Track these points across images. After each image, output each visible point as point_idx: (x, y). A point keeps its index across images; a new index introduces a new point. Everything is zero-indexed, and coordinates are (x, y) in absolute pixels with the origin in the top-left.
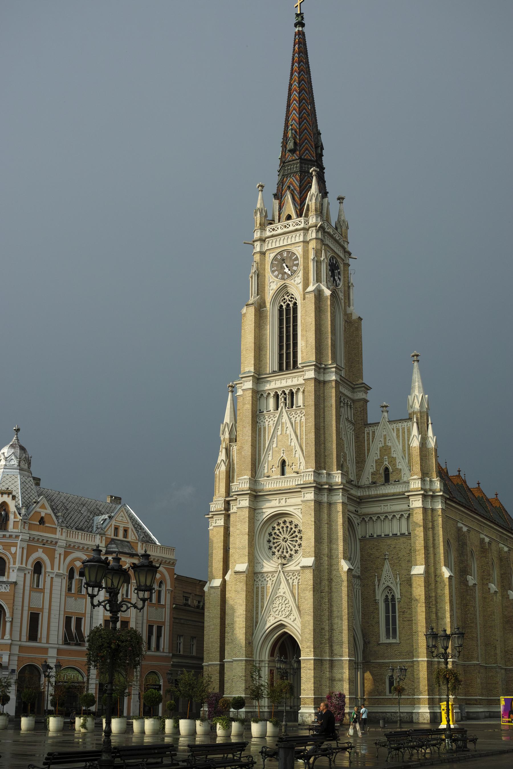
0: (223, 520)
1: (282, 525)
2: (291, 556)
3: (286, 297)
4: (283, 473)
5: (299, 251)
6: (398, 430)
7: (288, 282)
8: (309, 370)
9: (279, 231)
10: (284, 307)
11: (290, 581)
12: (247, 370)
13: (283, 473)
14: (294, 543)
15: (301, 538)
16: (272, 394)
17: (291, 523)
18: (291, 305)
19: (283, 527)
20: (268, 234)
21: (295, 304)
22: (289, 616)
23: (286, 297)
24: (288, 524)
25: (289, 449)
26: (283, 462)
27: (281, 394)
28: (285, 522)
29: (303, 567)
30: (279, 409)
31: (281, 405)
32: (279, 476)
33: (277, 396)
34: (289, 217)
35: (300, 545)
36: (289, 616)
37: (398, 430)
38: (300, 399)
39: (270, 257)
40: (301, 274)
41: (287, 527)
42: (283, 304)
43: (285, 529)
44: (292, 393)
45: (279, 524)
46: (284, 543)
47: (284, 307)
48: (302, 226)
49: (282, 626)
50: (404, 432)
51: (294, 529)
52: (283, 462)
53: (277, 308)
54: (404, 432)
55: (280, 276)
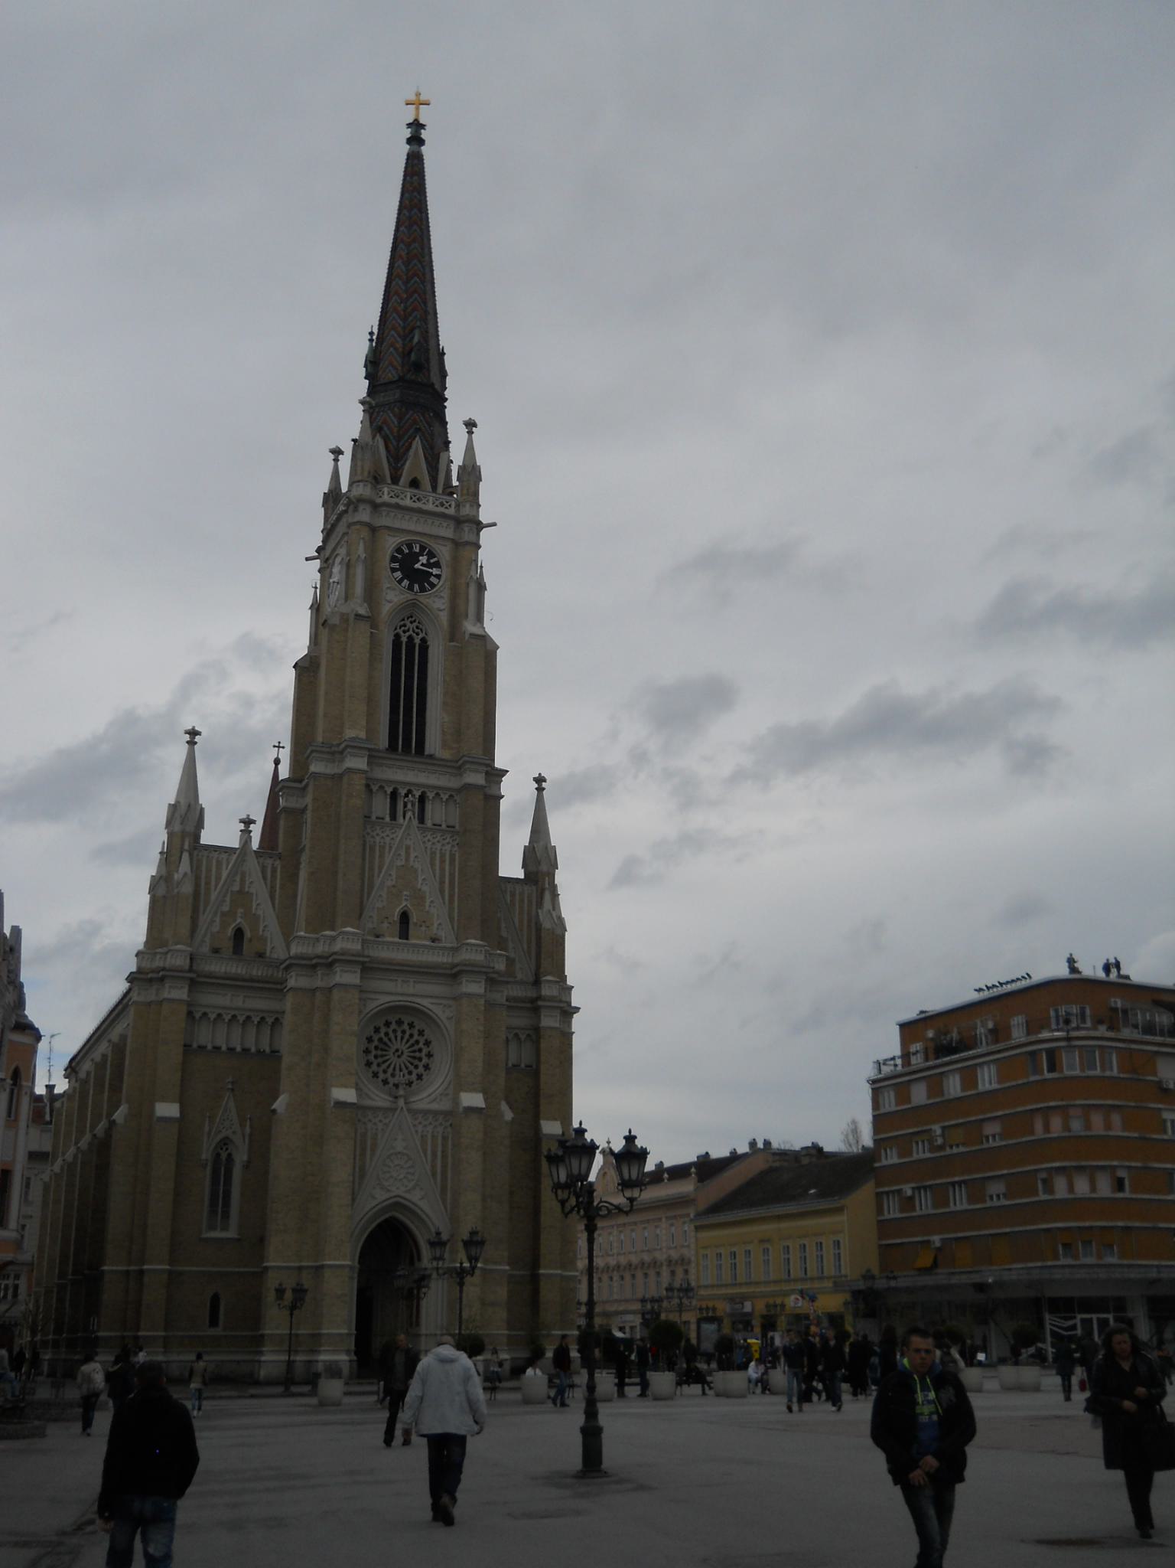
0: (186, 990)
1: (394, 1026)
2: (410, 1084)
3: (407, 622)
4: (404, 934)
5: (444, 552)
6: (513, 895)
7: (423, 598)
8: (477, 771)
9: (408, 502)
10: (404, 639)
11: (420, 1128)
12: (349, 733)
13: (404, 934)
14: (416, 1062)
15: (430, 1055)
16: (389, 790)
17: (411, 1025)
18: (417, 641)
19: (394, 1031)
20: (386, 498)
21: (424, 640)
22: (414, 1188)
23: (407, 622)
24: (406, 1027)
25: (419, 897)
26: (405, 917)
27: (406, 796)
28: (400, 1022)
29: (470, 1110)
30: (400, 820)
31: (409, 814)
32: (397, 940)
33: (394, 795)
34: (415, 483)
35: (427, 1067)
36: (414, 1188)
37: (513, 895)
38: (435, 813)
39: (390, 543)
40: (446, 594)
41: (404, 1032)
42: (400, 631)
43: (399, 1034)
44: (422, 799)
45: (388, 1024)
46: (394, 1059)
47: (404, 639)
48: (452, 511)
49: (397, 1206)
50: (522, 901)
51: (416, 1037)
52: (405, 917)
53: (392, 638)
54: (522, 901)
55: (406, 582)
